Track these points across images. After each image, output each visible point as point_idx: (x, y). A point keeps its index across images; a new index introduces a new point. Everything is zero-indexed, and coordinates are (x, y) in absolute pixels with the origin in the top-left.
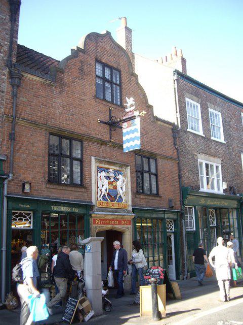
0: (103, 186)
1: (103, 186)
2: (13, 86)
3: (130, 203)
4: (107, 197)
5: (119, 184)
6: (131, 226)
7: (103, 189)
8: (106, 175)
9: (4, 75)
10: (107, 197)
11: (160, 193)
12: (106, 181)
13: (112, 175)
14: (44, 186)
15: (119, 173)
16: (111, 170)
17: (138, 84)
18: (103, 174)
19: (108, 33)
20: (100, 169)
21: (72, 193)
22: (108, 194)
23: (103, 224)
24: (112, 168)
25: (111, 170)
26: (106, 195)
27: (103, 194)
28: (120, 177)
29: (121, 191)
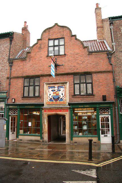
0: (50, 95)
1: (50, 95)
2: (10, 66)
3: (68, 101)
4: (53, 99)
5: (60, 93)
6: (68, 112)
7: (50, 96)
8: (52, 90)
9: (7, 64)
10: (53, 99)
11: (95, 93)
12: (52, 92)
13: (56, 89)
14: (21, 99)
15: (62, 87)
16: (56, 87)
17: (76, 39)
18: (51, 89)
19: (56, 24)
20: (50, 87)
21: (34, 100)
22: (53, 98)
23: (50, 112)
24: (56, 86)
25: (56, 87)
26: (53, 99)
27: (50, 98)
28: (62, 89)
29: (62, 96)
